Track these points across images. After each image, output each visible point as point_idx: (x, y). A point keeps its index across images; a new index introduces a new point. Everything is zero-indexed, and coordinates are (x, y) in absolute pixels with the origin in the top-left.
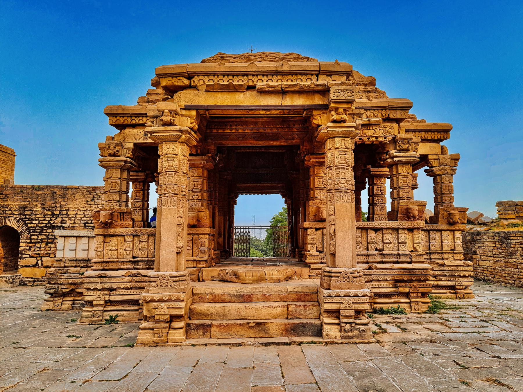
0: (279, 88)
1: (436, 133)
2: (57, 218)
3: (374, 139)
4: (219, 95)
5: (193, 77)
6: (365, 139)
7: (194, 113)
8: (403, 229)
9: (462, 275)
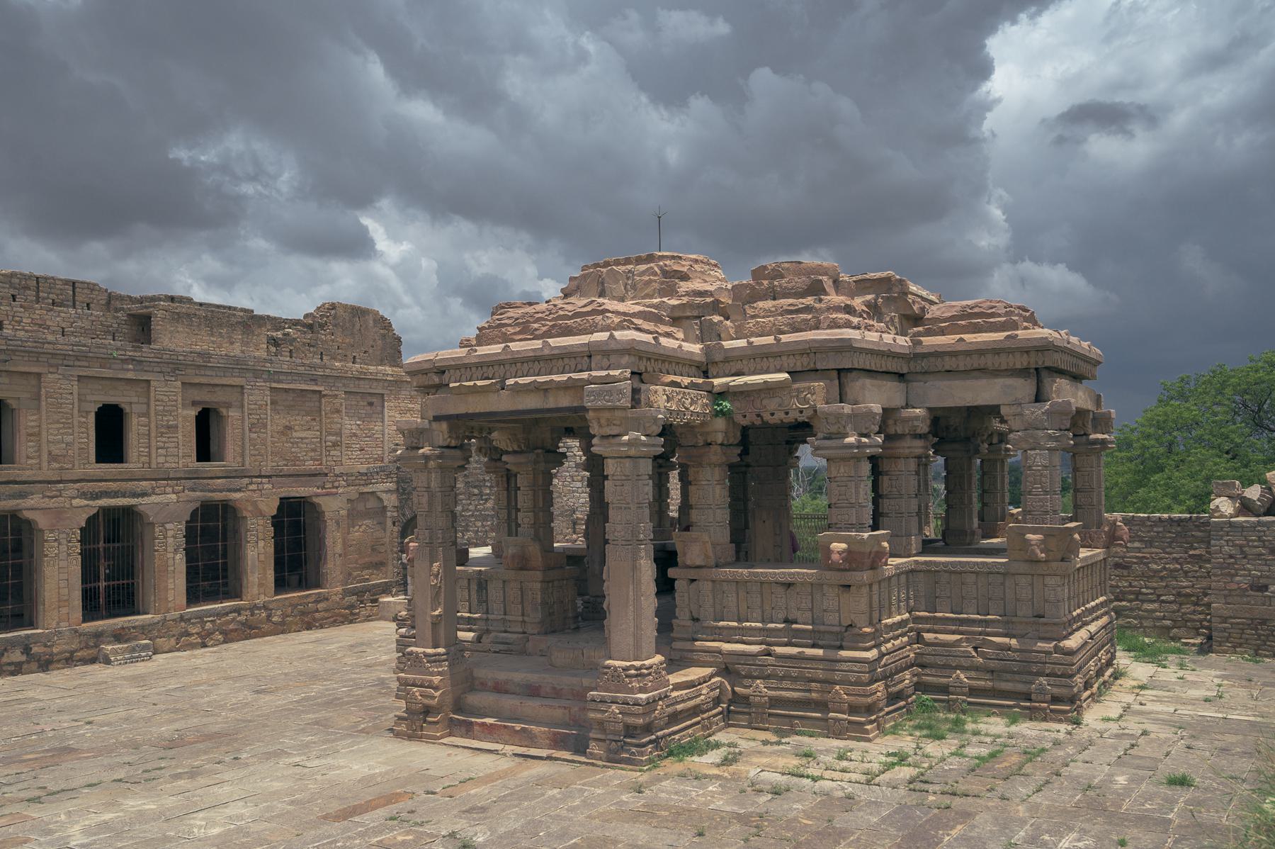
0: (532, 387)
1: (1018, 355)
2: (486, 500)
3: (782, 415)
4: (470, 399)
5: (444, 372)
6: (767, 417)
7: (444, 426)
8: (831, 586)
9: (1047, 671)
